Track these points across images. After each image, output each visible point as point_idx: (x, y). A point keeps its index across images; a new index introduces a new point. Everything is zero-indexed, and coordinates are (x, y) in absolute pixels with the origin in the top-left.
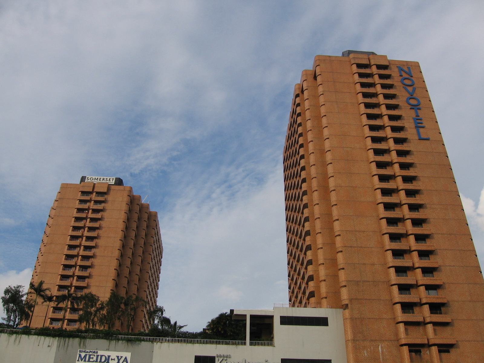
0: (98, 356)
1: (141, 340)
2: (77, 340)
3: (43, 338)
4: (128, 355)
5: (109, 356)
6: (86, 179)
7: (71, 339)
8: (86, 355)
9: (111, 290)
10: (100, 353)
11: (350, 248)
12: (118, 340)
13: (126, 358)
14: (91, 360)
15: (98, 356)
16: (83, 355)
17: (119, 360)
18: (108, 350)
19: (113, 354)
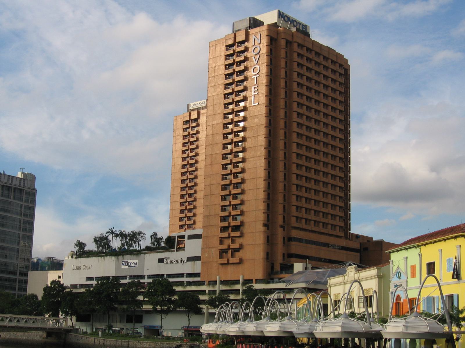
0: (128, 263)
1: (142, 253)
2: (121, 256)
3: (111, 257)
4: (136, 261)
5: (131, 262)
6: (190, 106)
7: (119, 256)
8: (124, 263)
9: (264, 169)
10: (129, 261)
11: (207, 196)
12: (135, 254)
13: (136, 263)
14: (126, 265)
15: (128, 263)
16: (123, 263)
17: (134, 264)
18: (131, 260)
19: (132, 261)
